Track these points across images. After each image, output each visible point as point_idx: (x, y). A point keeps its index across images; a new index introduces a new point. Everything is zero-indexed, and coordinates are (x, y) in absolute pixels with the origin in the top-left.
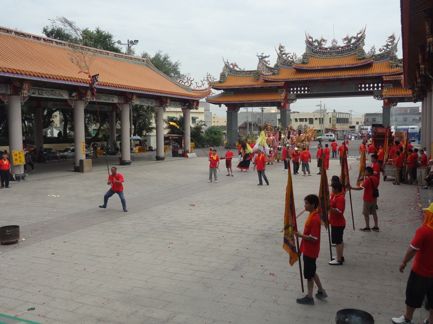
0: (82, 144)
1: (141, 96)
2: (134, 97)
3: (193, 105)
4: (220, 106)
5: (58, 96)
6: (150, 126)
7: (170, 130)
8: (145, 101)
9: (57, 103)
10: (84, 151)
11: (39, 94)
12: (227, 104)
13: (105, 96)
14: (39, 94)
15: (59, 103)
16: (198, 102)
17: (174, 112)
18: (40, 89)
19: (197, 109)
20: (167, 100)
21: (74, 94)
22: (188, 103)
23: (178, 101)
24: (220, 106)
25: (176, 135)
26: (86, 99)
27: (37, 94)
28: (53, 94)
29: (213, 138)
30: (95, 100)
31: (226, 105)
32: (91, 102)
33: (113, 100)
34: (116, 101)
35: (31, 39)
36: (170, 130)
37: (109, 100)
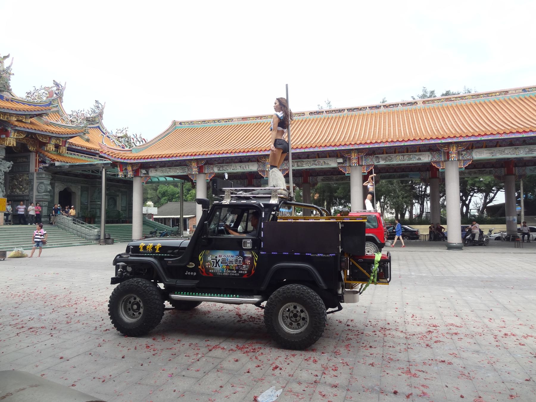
8: (506, 152)
11: (298, 166)
13: (404, 155)
14: (298, 166)
30: (382, 162)
33: (420, 159)
35: (368, 110)
37: (410, 159)
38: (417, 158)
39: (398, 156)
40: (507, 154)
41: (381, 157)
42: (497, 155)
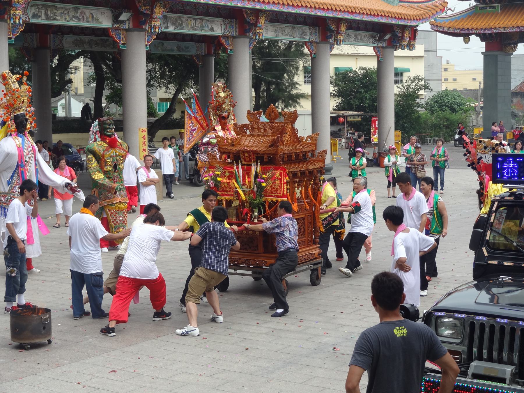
0: (142, 135)
1: (277, 18)
2: (262, 22)
3: (402, 38)
4: (467, 41)
5: (88, 22)
6: (294, 92)
7: (340, 100)
8: (287, 32)
9: (83, 37)
10: (144, 150)
11: (47, 18)
12: (484, 34)
13: (195, 19)
14: (47, 18)
15: (86, 39)
16: (414, 31)
17: (354, 56)
18: (49, 6)
19: (411, 47)
20: (338, 27)
21: (124, 17)
22: (389, 34)
23: (366, 30)
24: (467, 41)
25: (355, 113)
26: (151, 27)
27: (43, 17)
28: (77, 18)
29: (447, 120)
30: (171, 29)
31: (483, 37)
32: (162, 33)
33: (212, 29)
34: (217, 29)
36: (340, 100)
37: (202, 28)
38: (210, 27)
39: (189, 20)
40: (287, 35)
41: (171, 18)
42: (280, 34)
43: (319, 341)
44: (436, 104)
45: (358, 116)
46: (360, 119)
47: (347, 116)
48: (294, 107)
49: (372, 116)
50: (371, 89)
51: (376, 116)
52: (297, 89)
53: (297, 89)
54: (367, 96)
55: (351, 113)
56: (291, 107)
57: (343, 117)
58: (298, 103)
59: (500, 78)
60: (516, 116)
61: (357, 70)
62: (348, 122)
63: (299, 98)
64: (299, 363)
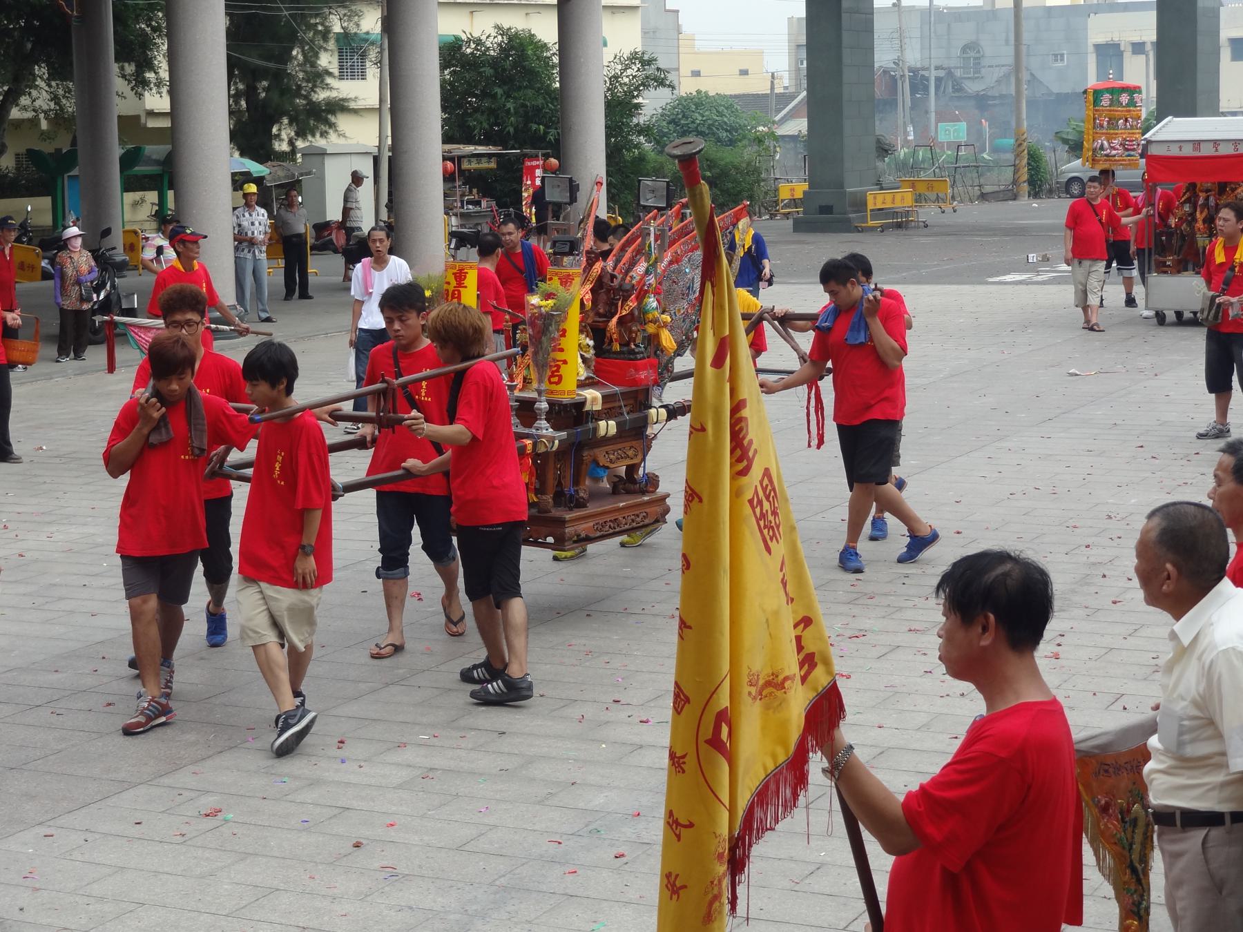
6: (321, 96)
25: (481, 149)
43: (582, 805)
44: (672, 127)
45: (490, 156)
46: (493, 165)
47: (460, 158)
48: (322, 135)
49: (525, 155)
50: (520, 88)
51: (536, 157)
52: (328, 87)
53: (328, 87)
54: (510, 105)
55: (470, 149)
56: (314, 136)
57: (452, 159)
58: (332, 125)
59: (846, 53)
60: (886, 151)
61: (483, 38)
62: (462, 172)
63: (333, 113)
64: (544, 888)
